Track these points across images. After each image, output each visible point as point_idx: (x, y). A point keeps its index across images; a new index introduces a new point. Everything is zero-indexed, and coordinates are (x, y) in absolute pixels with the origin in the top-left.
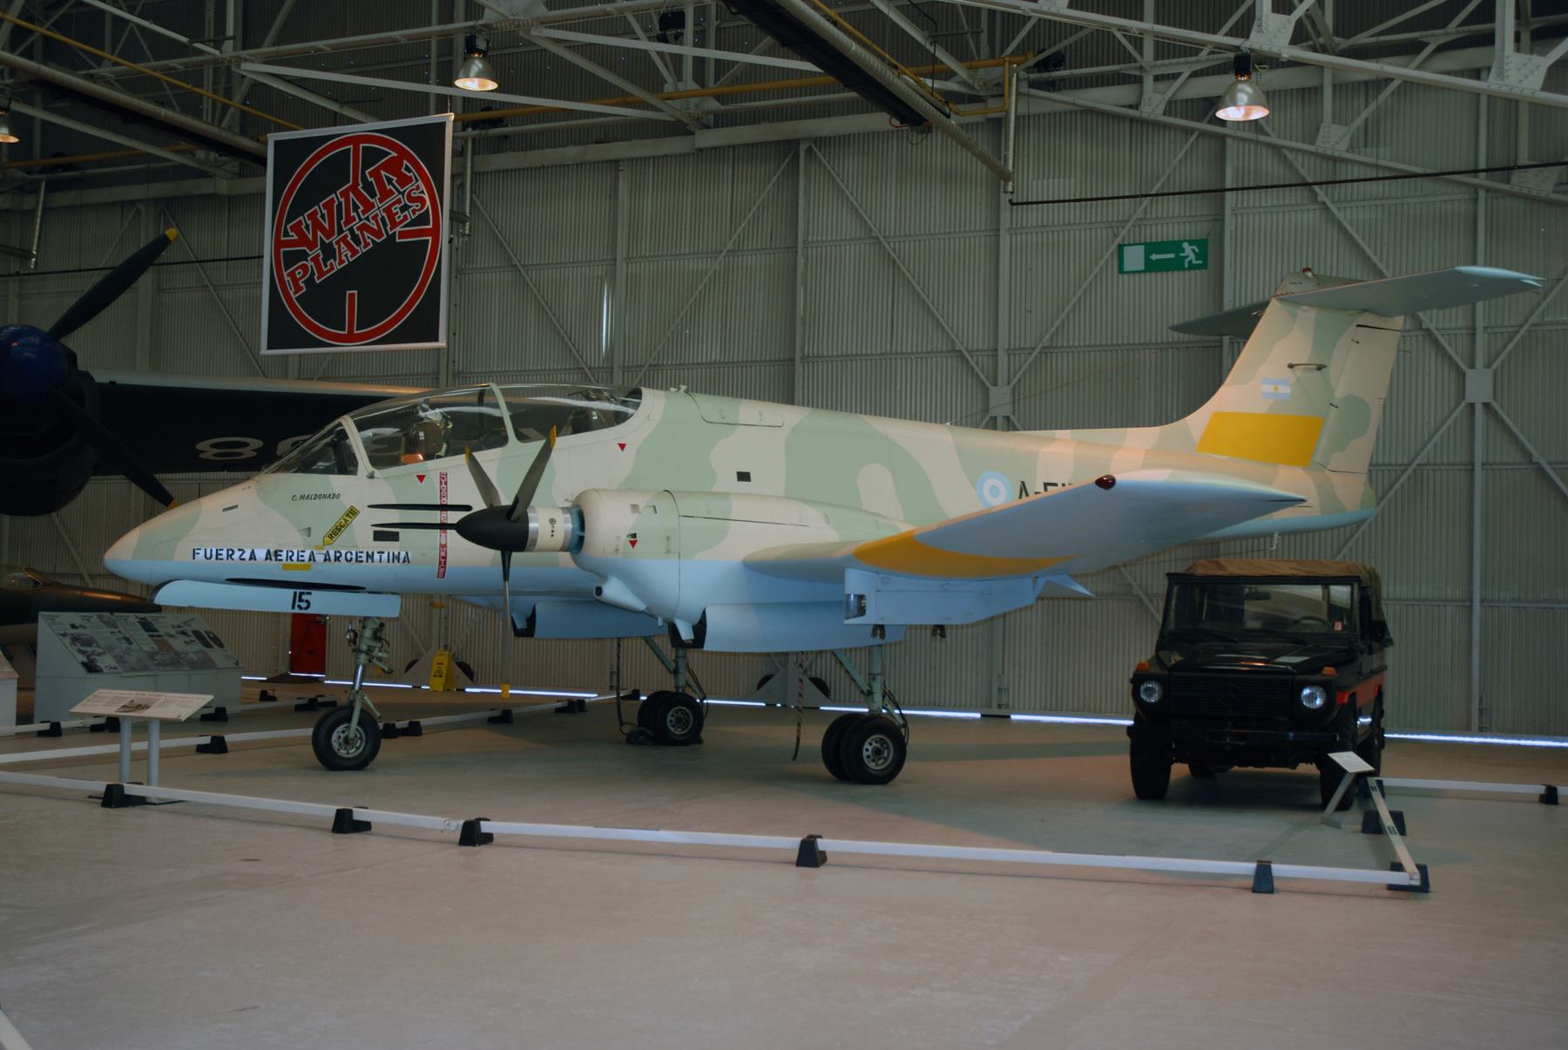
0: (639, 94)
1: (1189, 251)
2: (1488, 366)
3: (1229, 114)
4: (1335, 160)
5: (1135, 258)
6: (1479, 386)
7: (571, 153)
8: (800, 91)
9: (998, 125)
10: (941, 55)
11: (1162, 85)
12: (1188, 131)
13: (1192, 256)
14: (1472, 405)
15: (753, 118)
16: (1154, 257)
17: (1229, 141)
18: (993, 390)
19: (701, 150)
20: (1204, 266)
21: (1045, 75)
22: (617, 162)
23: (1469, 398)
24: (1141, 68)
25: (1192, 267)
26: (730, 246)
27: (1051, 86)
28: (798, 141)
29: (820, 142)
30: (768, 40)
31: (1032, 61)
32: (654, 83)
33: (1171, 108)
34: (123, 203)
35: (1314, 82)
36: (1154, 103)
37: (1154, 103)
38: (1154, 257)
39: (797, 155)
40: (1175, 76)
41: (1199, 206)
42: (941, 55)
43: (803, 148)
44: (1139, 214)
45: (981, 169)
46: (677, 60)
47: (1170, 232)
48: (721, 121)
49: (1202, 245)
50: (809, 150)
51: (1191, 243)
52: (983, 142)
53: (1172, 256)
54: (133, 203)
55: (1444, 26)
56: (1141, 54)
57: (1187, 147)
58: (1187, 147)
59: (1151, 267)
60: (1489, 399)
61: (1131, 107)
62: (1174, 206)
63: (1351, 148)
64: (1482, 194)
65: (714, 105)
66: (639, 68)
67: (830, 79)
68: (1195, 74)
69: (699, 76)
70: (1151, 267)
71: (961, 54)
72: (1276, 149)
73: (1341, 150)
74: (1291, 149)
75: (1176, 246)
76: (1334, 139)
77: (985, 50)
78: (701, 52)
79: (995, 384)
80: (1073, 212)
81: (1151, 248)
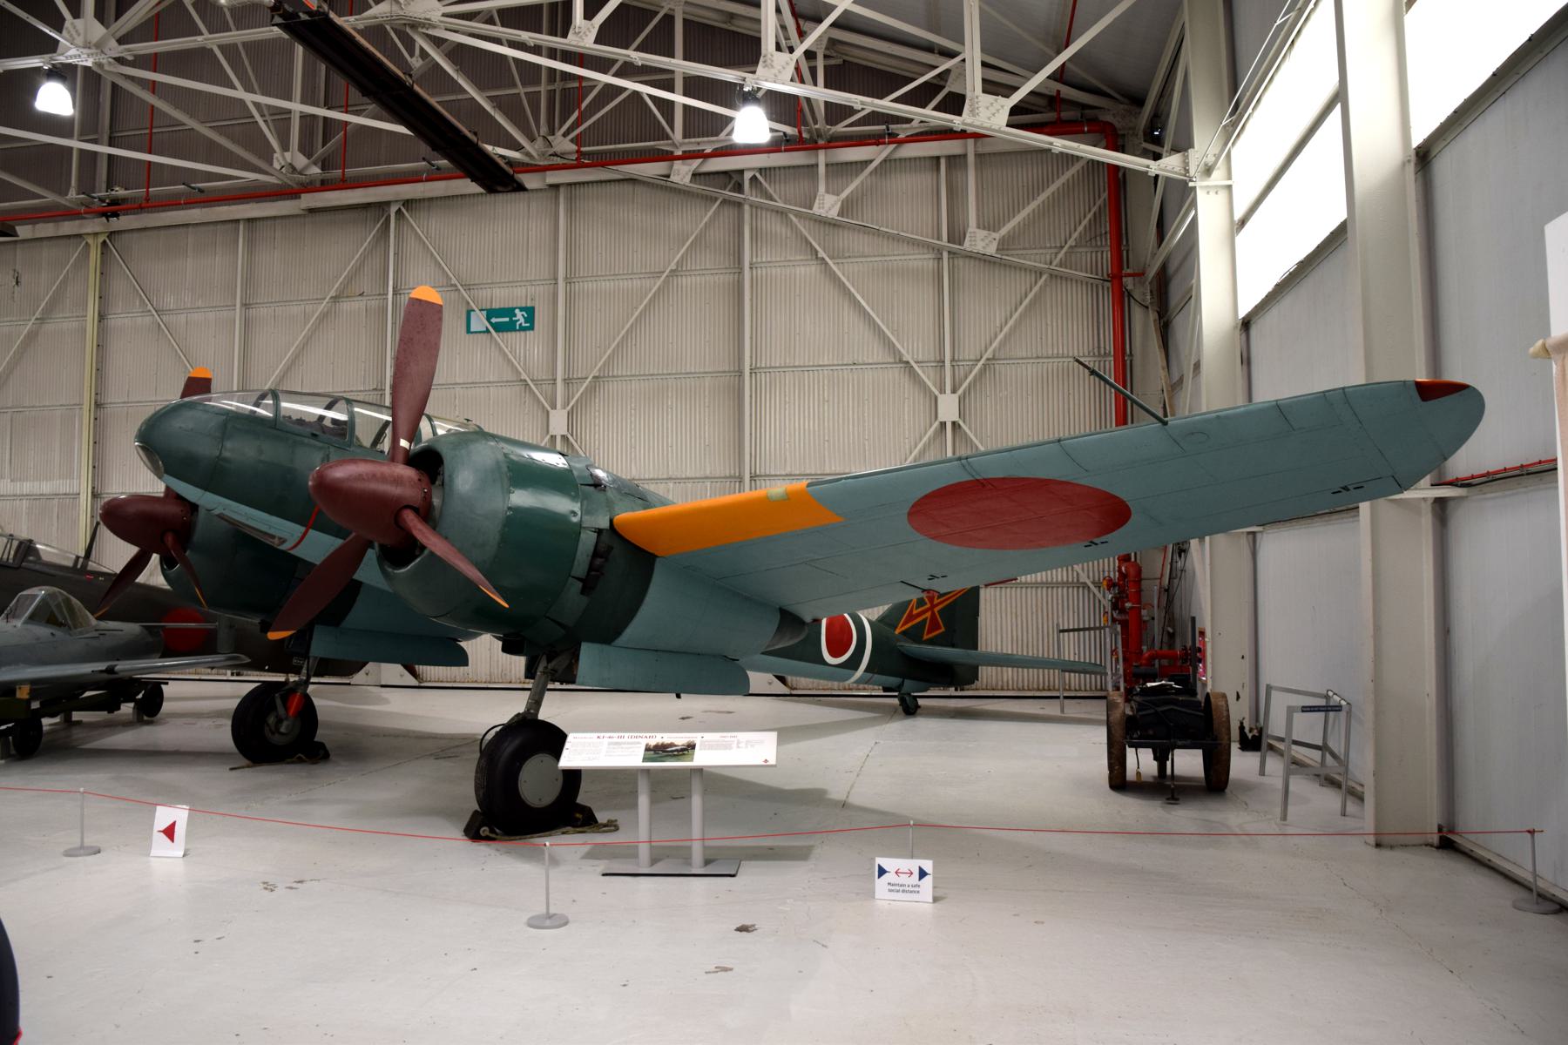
2: (954, 391)
4: (832, 224)
6: (948, 408)
14: (943, 425)
17: (747, 207)
18: (552, 413)
22: (237, 221)
23: (941, 418)
24: (674, 145)
28: (388, 203)
29: (408, 203)
35: (812, 162)
43: (393, 209)
48: (325, 185)
50: (399, 212)
56: (672, 129)
60: (956, 418)
63: (841, 214)
64: (945, 255)
72: (782, 213)
73: (833, 214)
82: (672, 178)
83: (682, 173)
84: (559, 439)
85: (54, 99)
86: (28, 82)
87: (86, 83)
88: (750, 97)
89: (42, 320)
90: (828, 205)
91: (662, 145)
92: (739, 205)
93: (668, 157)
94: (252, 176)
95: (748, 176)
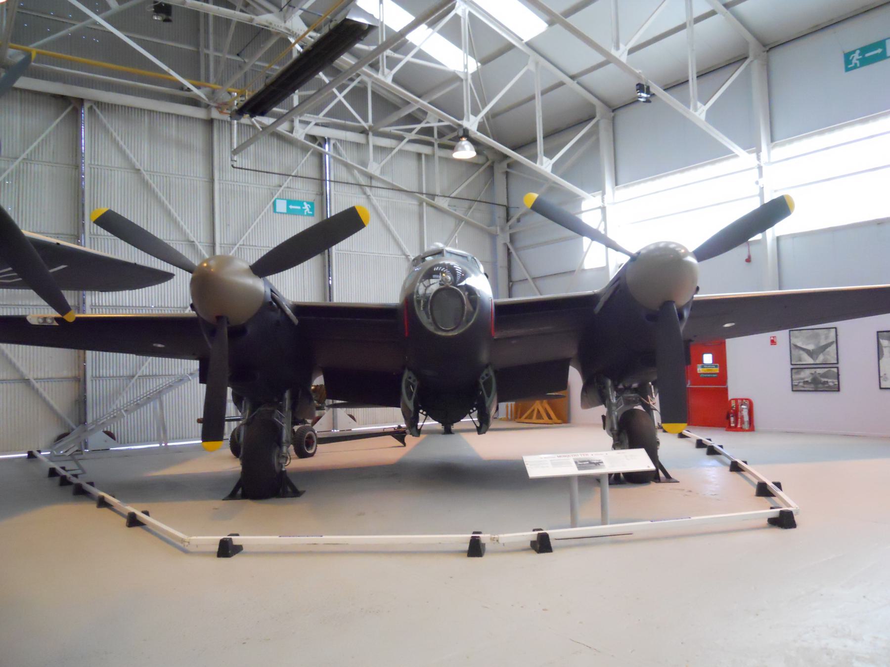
1: (307, 207)
3: (457, 155)
4: (371, 177)
5: (282, 206)
11: (303, 125)
13: (308, 210)
16: (291, 207)
20: (313, 215)
25: (308, 215)
26: (24, 156)
29: (99, 104)
36: (300, 133)
37: (300, 133)
38: (291, 207)
40: (308, 123)
43: (87, 105)
47: (297, 196)
49: (312, 204)
50: (91, 108)
51: (308, 203)
53: (299, 208)
59: (290, 212)
62: (299, 184)
68: (317, 124)
70: (290, 212)
73: (377, 173)
75: (300, 203)
76: (374, 168)
80: (250, 177)
81: (290, 202)
95: (332, 142)
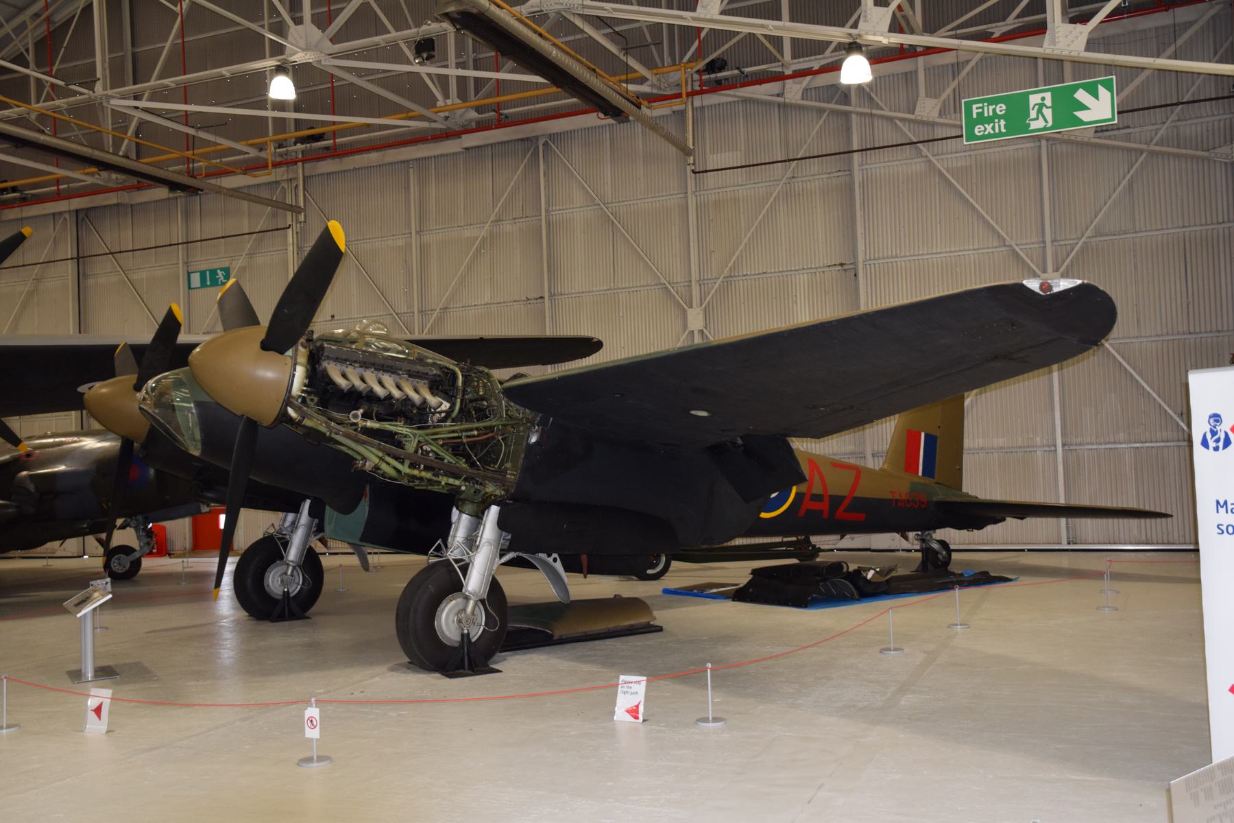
0: (418, 110)
4: (932, 125)
7: (373, 157)
8: (538, 100)
9: (683, 113)
10: (632, 62)
12: (820, 111)
15: (501, 123)
17: (854, 116)
18: (690, 311)
19: (467, 149)
21: (713, 76)
22: (408, 161)
27: (719, 86)
28: (537, 138)
29: (552, 136)
30: (511, 64)
31: (701, 65)
32: (430, 102)
33: (806, 93)
34: (54, 214)
39: (537, 148)
41: (831, 164)
42: (632, 62)
43: (541, 142)
44: (789, 174)
45: (672, 150)
46: (443, 81)
48: (481, 127)
50: (546, 144)
52: (672, 129)
54: (61, 213)
55: (1004, 20)
57: (821, 122)
58: (821, 122)
61: (778, 95)
63: (940, 115)
65: (473, 115)
66: (414, 88)
67: (554, 89)
69: (463, 95)
71: (650, 64)
73: (934, 116)
74: (902, 120)
77: (667, 60)
78: (461, 72)
79: (691, 307)
82: (786, 95)
83: (794, 91)
84: (696, 333)
85: (282, 89)
86: (260, 81)
87: (300, 74)
88: (853, 47)
89: (250, 255)
90: (928, 108)
91: (774, 68)
92: (847, 114)
93: (780, 77)
94: (425, 125)
